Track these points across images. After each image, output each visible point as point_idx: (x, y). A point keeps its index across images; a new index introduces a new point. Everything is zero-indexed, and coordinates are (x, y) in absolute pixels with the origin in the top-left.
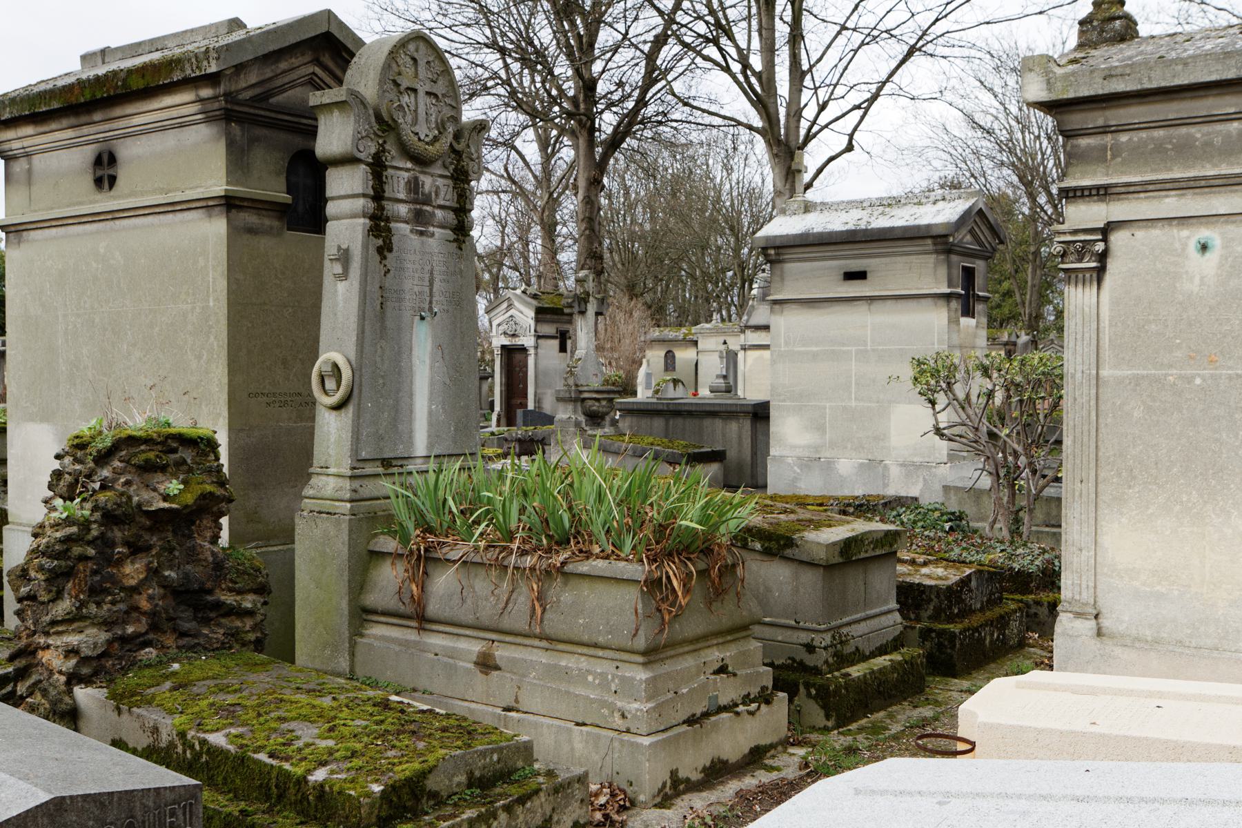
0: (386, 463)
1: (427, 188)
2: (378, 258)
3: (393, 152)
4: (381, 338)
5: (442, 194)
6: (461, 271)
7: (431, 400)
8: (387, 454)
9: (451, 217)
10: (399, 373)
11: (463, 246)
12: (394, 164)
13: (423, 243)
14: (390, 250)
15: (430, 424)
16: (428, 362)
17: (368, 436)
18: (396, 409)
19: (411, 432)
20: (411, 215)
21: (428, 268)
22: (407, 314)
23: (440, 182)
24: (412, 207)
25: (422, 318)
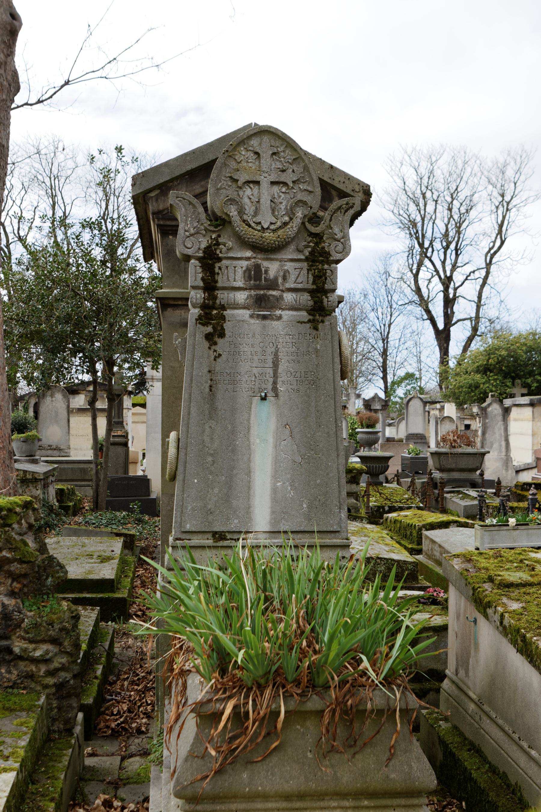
0: (219, 536)
1: (272, 274)
2: (206, 344)
3: (230, 244)
4: (211, 418)
5: (293, 278)
6: (317, 351)
7: (275, 476)
8: (218, 528)
9: (305, 299)
10: (233, 451)
11: (320, 326)
12: (231, 255)
13: (264, 327)
14: (222, 335)
15: (274, 500)
16: (271, 440)
17: (193, 509)
18: (229, 485)
19: (248, 509)
20: (250, 301)
21: (271, 350)
22: (243, 395)
23: (289, 266)
24: (253, 293)
25: (264, 399)
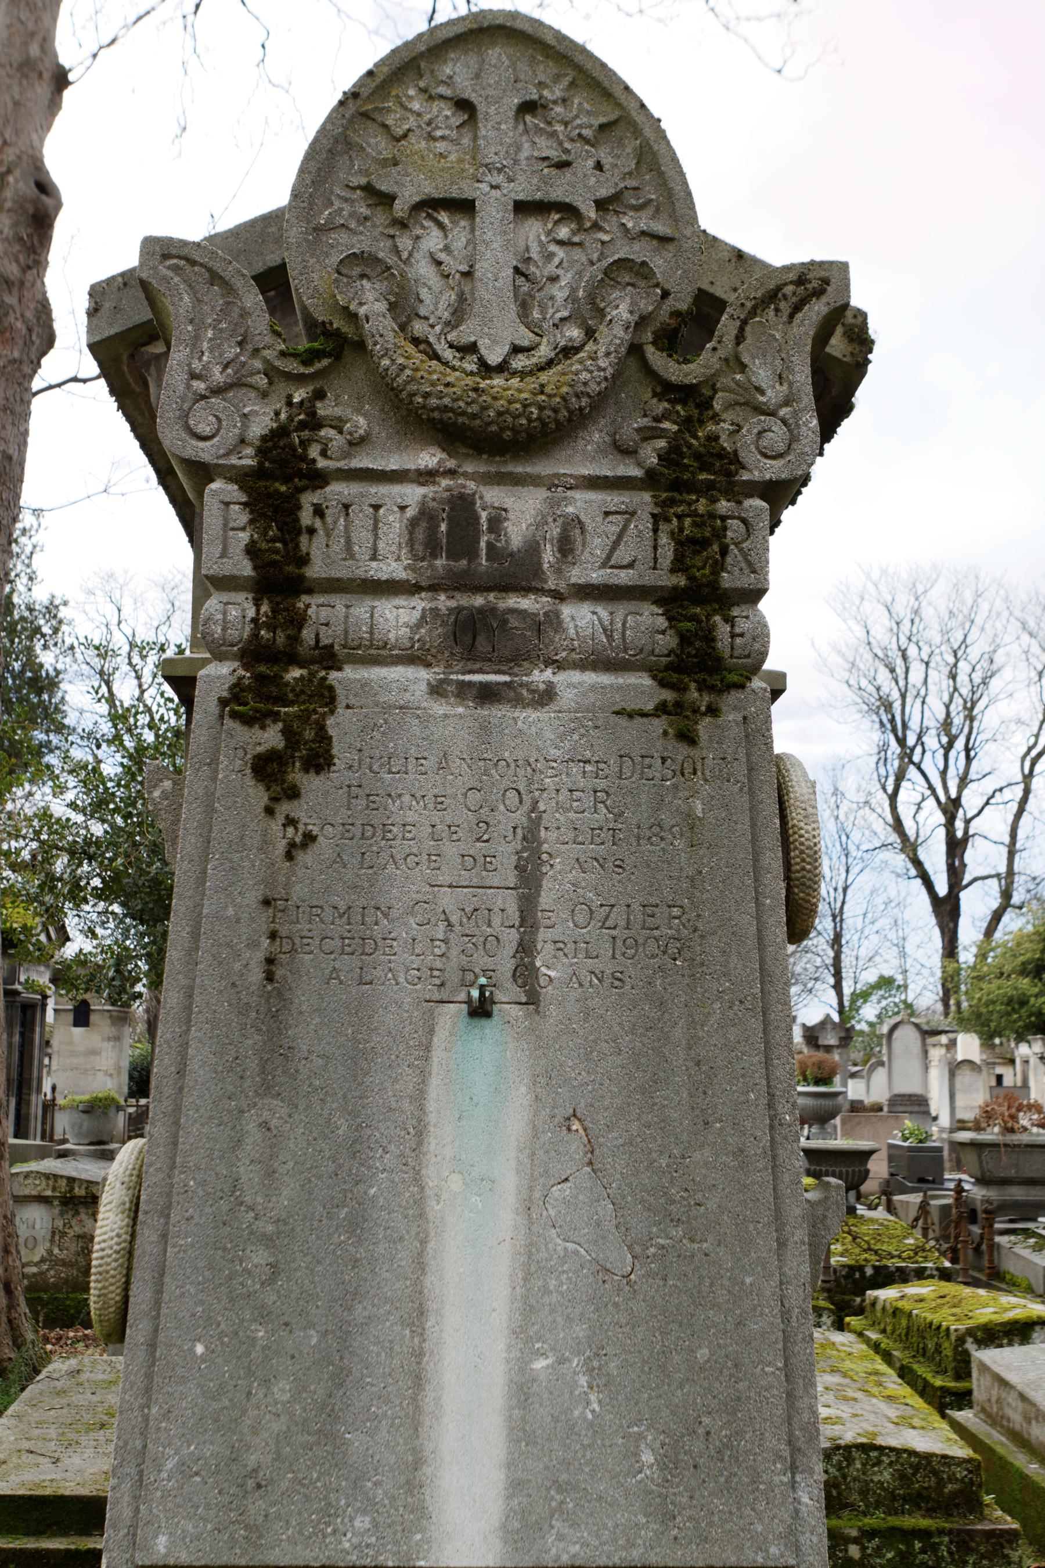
2: (258, 796)
4: (267, 1088)
5: (597, 546)
6: (692, 823)
7: (526, 1333)
10: (356, 1225)
11: (704, 727)
13: (485, 728)
14: (320, 760)
15: (522, 1435)
17: (185, 1471)
18: (337, 1368)
19: (413, 1473)
20: (433, 635)
21: (509, 818)
22: (399, 994)
23: (583, 503)
24: (444, 602)
25: (481, 1010)
